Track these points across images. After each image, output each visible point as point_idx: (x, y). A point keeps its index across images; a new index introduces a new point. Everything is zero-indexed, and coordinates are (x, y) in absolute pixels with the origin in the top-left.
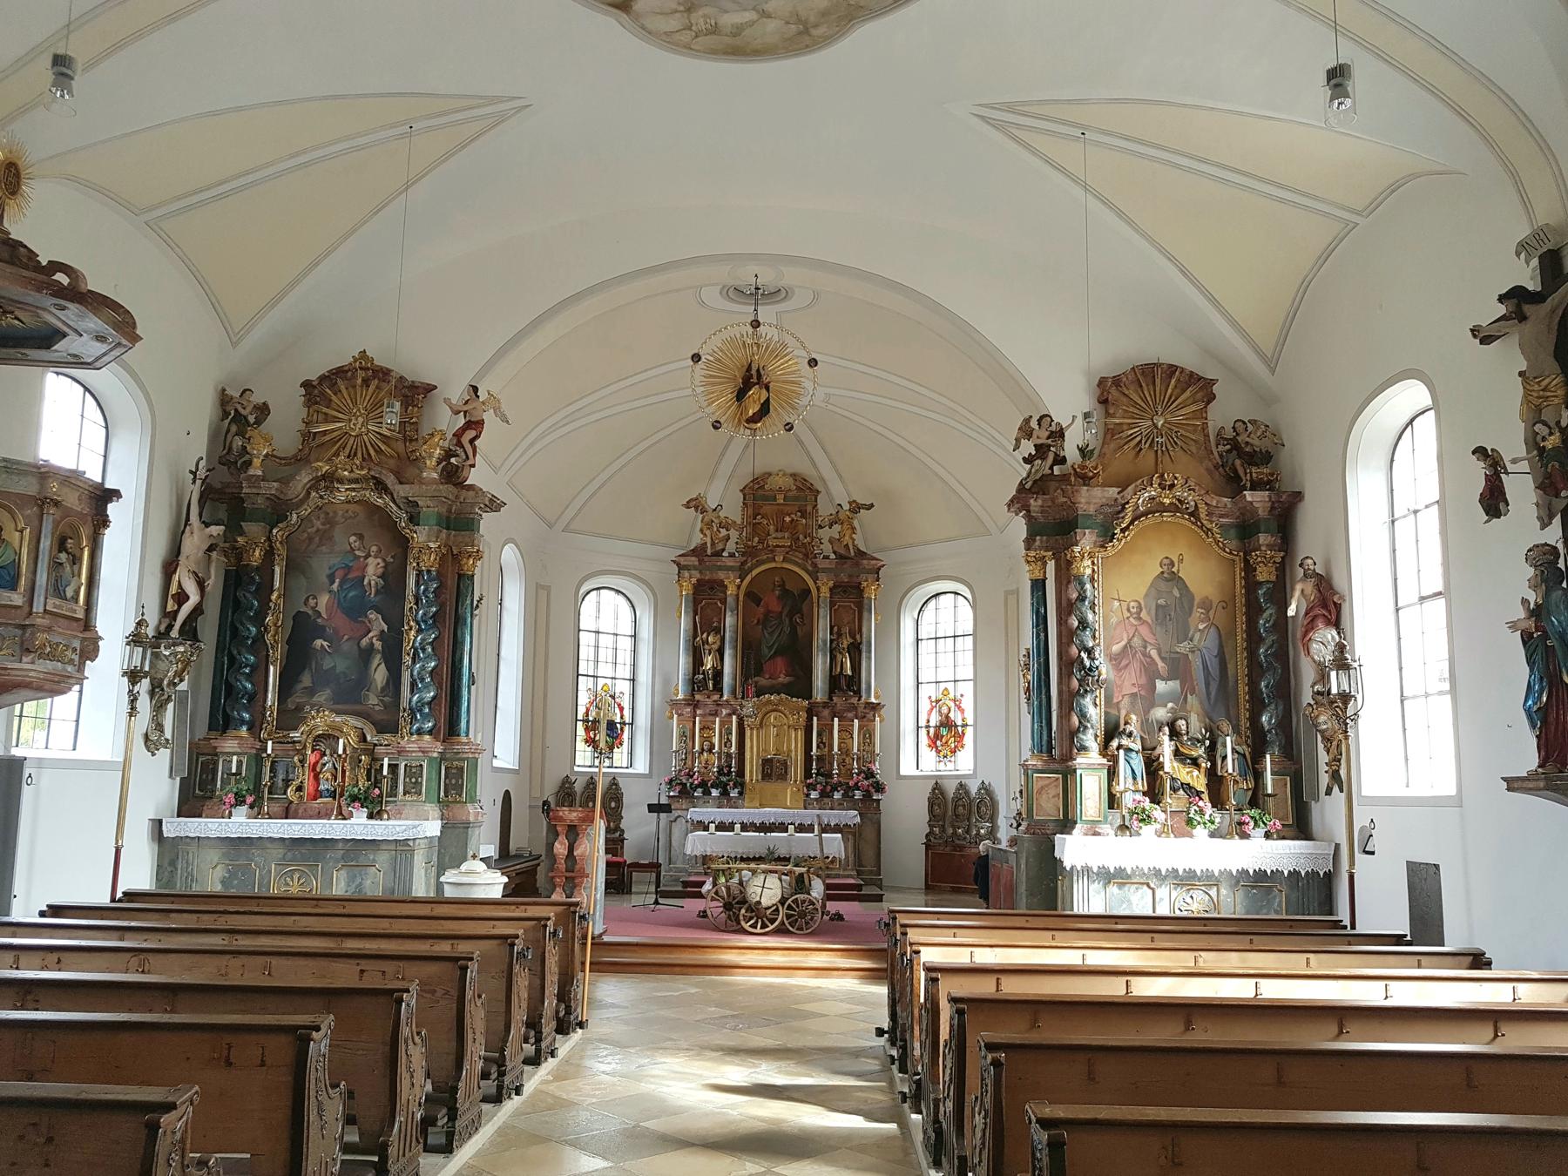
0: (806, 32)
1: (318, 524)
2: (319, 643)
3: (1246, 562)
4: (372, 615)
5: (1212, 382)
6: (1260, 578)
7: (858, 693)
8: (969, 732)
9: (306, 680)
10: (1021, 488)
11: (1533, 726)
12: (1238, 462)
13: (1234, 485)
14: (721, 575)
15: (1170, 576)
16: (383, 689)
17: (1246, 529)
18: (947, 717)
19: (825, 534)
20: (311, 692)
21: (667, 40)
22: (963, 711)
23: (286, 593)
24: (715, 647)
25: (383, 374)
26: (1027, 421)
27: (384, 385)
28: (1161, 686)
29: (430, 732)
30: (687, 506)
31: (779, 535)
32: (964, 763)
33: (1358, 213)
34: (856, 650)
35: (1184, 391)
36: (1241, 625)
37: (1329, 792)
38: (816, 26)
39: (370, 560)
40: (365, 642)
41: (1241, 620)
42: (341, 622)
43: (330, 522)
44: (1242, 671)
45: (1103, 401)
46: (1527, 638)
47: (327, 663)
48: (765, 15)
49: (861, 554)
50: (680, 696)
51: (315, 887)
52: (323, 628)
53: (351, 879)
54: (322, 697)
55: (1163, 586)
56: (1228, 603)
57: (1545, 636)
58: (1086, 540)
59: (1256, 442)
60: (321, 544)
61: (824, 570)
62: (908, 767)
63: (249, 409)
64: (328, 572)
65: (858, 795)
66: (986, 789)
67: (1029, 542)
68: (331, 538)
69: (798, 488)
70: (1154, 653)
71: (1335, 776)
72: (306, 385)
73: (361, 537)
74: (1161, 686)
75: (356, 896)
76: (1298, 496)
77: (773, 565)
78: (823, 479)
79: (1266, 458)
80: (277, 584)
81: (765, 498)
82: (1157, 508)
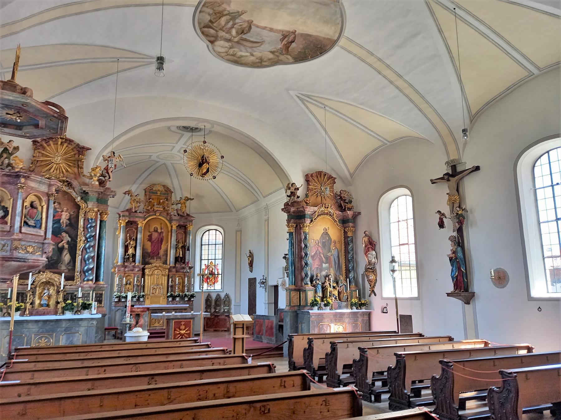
0: (261, 63)
3: (345, 230)
4: (64, 234)
5: (335, 178)
6: (349, 235)
7: (184, 263)
8: (220, 276)
10: (286, 204)
11: (453, 280)
12: (342, 202)
13: (341, 208)
14: (137, 219)
15: (326, 234)
17: (344, 222)
18: (212, 271)
19: (175, 207)
21: (219, 55)
22: (218, 270)
24: (134, 245)
26: (289, 184)
27: (70, 146)
28: (324, 265)
29: (92, 280)
30: (125, 193)
31: (158, 206)
32: (218, 286)
33: (389, 142)
34: (185, 248)
35: (328, 180)
36: (343, 249)
37: (370, 296)
38: (265, 62)
39: (63, 213)
40: (60, 245)
41: (343, 247)
44: (344, 261)
45: (307, 181)
46: (451, 259)
48: (252, 55)
49: (188, 215)
50: (119, 264)
51: (52, 342)
53: (68, 339)
55: (324, 235)
56: (340, 242)
57: (456, 258)
58: (308, 221)
59: (345, 196)
61: (175, 220)
62: (197, 289)
63: (12, 148)
65: (186, 299)
66: (227, 296)
67: (288, 221)
69: (165, 190)
70: (322, 256)
71: (373, 291)
73: (59, 204)
74: (324, 265)
75: (70, 345)
76: (359, 213)
77: (155, 217)
78: (174, 188)
79: (351, 202)
81: (153, 193)
82: (323, 214)
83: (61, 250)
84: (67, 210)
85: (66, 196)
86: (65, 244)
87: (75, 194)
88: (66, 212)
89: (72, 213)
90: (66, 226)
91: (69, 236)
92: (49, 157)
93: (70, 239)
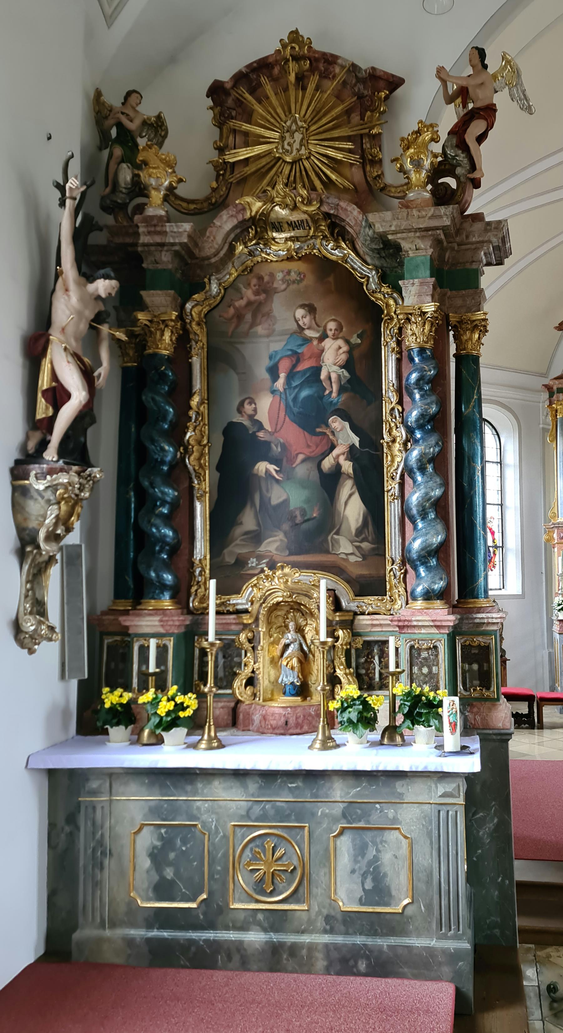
1: (249, 294)
2: (262, 467)
4: (336, 423)
9: (248, 521)
16: (359, 532)
20: (256, 538)
23: (210, 398)
39: (328, 344)
40: (327, 463)
43: (266, 290)
47: (277, 495)
52: (267, 444)
54: (273, 545)
60: (253, 324)
64: (266, 362)
68: (268, 315)
73: (311, 309)
80: (198, 384)
83: (330, 481)
84: (340, 328)
85: (331, 279)
86: (342, 460)
87: (358, 263)
88: (335, 338)
89: (355, 340)
90: (342, 389)
91: (354, 429)
93: (356, 440)
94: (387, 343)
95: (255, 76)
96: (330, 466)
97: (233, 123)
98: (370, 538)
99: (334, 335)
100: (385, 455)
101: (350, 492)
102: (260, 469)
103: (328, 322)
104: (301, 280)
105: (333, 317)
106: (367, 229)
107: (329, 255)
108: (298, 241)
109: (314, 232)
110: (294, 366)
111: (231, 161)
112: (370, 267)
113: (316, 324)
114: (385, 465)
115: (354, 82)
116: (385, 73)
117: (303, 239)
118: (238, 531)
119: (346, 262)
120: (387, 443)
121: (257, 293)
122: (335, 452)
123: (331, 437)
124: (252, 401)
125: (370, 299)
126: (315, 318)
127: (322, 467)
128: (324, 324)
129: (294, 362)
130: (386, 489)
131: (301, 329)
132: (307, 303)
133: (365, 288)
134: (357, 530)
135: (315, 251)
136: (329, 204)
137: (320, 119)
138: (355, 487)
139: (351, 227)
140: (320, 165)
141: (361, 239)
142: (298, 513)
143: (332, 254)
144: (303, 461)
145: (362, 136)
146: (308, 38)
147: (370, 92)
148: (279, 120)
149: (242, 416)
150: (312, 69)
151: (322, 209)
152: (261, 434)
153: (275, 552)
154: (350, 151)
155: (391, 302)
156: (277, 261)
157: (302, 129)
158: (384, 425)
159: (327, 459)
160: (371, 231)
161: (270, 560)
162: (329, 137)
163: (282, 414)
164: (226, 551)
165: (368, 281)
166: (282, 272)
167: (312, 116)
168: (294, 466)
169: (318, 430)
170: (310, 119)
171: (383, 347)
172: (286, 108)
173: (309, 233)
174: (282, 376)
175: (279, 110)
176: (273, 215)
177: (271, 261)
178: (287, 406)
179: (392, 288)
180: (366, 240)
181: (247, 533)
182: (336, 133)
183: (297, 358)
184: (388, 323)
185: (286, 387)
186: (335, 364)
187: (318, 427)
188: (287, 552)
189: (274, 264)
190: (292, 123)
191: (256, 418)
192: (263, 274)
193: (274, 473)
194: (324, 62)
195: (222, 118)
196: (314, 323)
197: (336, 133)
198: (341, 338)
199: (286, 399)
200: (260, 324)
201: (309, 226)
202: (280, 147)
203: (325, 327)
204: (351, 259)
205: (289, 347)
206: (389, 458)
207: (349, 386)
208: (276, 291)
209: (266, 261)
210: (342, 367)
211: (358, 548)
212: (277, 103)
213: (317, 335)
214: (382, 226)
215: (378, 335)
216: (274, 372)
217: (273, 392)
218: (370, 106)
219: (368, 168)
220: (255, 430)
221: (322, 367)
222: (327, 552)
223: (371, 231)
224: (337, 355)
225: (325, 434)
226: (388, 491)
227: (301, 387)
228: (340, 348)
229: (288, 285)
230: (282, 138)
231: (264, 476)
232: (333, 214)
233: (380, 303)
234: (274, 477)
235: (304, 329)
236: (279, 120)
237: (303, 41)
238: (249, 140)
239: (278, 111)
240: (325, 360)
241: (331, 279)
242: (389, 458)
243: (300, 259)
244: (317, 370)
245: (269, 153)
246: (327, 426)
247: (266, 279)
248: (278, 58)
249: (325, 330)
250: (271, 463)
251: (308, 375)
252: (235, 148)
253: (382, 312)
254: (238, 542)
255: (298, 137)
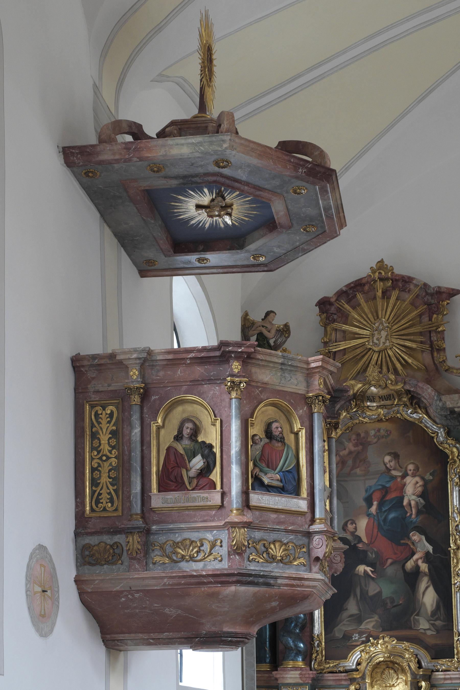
2: (361, 568)
4: (415, 537)
9: (352, 607)
16: (434, 613)
25: (402, 283)
39: (408, 480)
40: (410, 565)
42: (383, 545)
47: (373, 589)
60: (354, 467)
64: (363, 494)
72: (324, 304)
73: (396, 456)
83: (412, 578)
85: (410, 434)
86: (420, 562)
87: (430, 423)
88: (414, 476)
89: (428, 477)
90: (419, 512)
91: (429, 540)
92: (355, 336)
93: (430, 548)
94: (452, 479)
95: (351, 292)
96: (411, 567)
97: (335, 325)
98: (442, 618)
99: (413, 474)
100: (452, 558)
101: (426, 586)
102: (360, 570)
103: (408, 465)
104: (388, 435)
105: (412, 461)
106: (438, 402)
107: (408, 418)
108: (386, 408)
109: (398, 402)
110: (384, 496)
111: (333, 350)
112: (439, 426)
113: (400, 466)
114: (452, 566)
115: (424, 294)
116: (447, 288)
117: (389, 407)
118: (345, 615)
119: (421, 422)
120: (454, 550)
121: (356, 445)
122: (415, 557)
123: (412, 546)
124: (353, 522)
125: (439, 448)
126: (398, 462)
127: (405, 568)
128: (405, 466)
129: (384, 493)
130: (453, 583)
131: (388, 470)
132: (393, 451)
133: (435, 440)
134: (432, 612)
135: (398, 415)
136: (410, 384)
137: (399, 321)
138: (430, 581)
139: (425, 399)
140: (400, 353)
141: (434, 408)
142: (388, 601)
143: (411, 417)
144: (391, 564)
145: (430, 332)
146: (391, 266)
147: (436, 302)
148: (370, 323)
149: (346, 533)
150: (394, 287)
151: (405, 388)
152: (360, 545)
153: (372, 629)
154: (421, 342)
155: (455, 450)
156: (370, 422)
157: (386, 329)
158: (451, 538)
159: (409, 562)
160: (441, 403)
161: (368, 635)
162: (406, 333)
163: (376, 530)
164: (336, 629)
165: (437, 435)
166: (374, 430)
167: (394, 320)
168: (385, 567)
169: (402, 541)
170: (392, 321)
171: (449, 482)
172: (375, 314)
173: (394, 402)
174: (375, 503)
175: (370, 316)
176: (369, 392)
177: (366, 423)
178: (379, 524)
179: (456, 440)
180: (437, 409)
181: (351, 616)
182: (411, 330)
183: (385, 491)
184: (453, 465)
185: (378, 511)
186: (414, 495)
187: (402, 539)
188: (381, 630)
189: (368, 424)
190: (380, 325)
191: (356, 534)
192: (360, 432)
193: (370, 573)
194: (402, 282)
195: (328, 321)
196: (398, 465)
197: (411, 330)
198: (418, 476)
199: (378, 520)
200: (358, 467)
201: (394, 398)
202: (371, 341)
203: (406, 468)
204: (425, 421)
205: (380, 483)
206: (455, 561)
207: (424, 510)
208: (369, 444)
209: (362, 422)
210: (418, 496)
211: (433, 625)
212: (369, 311)
213: (400, 474)
214: (451, 403)
215: (445, 473)
216: (369, 501)
217: (369, 515)
218: (436, 311)
219: (435, 354)
220: (356, 542)
221: (404, 496)
222: (411, 628)
223: (441, 403)
224: (415, 488)
225: (407, 544)
226: (455, 584)
227: (389, 510)
228: (417, 483)
229: (379, 439)
230: (373, 335)
231: (363, 575)
232: (413, 391)
233: (447, 451)
234: (370, 576)
235: (390, 470)
236: (370, 323)
237: (387, 268)
238: (346, 336)
239: (369, 316)
240: (407, 491)
241: (410, 434)
242: (455, 561)
243: (387, 420)
244: (402, 498)
245: (363, 345)
246: (409, 538)
247: (362, 435)
248: (369, 280)
249: (406, 470)
250: (368, 566)
251: (394, 502)
252: (336, 342)
253: (448, 457)
254: (344, 622)
255: (384, 334)
